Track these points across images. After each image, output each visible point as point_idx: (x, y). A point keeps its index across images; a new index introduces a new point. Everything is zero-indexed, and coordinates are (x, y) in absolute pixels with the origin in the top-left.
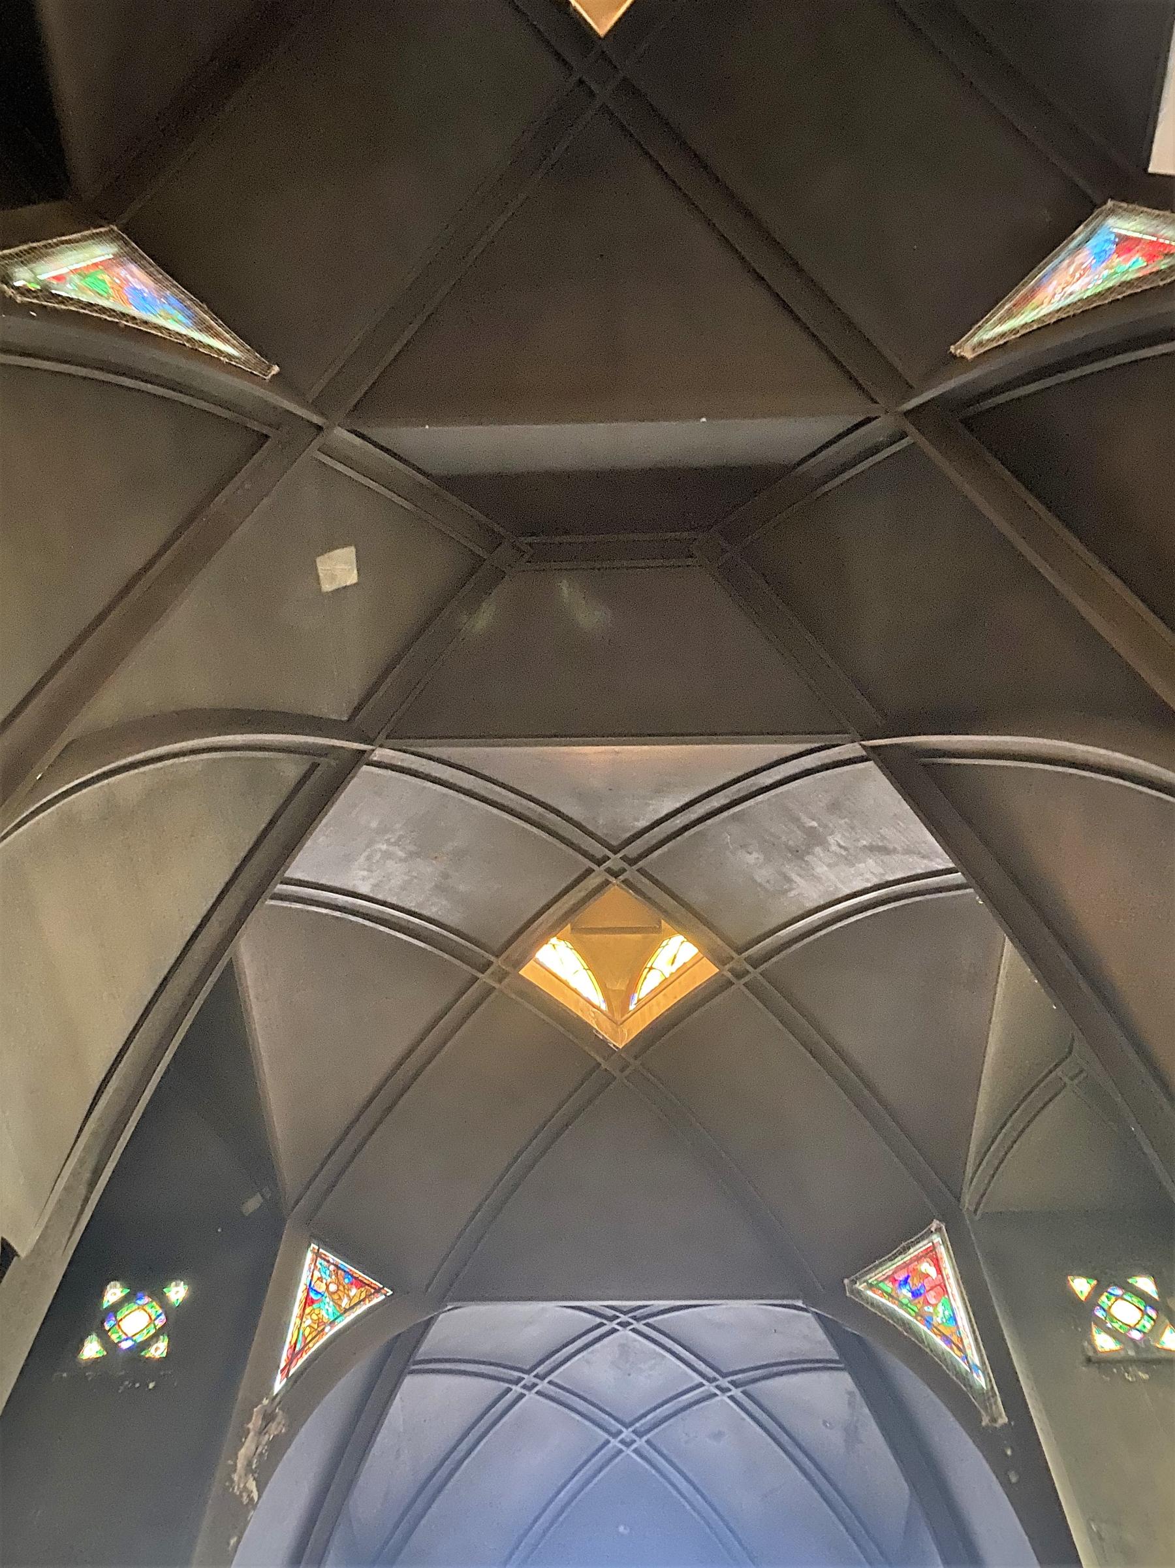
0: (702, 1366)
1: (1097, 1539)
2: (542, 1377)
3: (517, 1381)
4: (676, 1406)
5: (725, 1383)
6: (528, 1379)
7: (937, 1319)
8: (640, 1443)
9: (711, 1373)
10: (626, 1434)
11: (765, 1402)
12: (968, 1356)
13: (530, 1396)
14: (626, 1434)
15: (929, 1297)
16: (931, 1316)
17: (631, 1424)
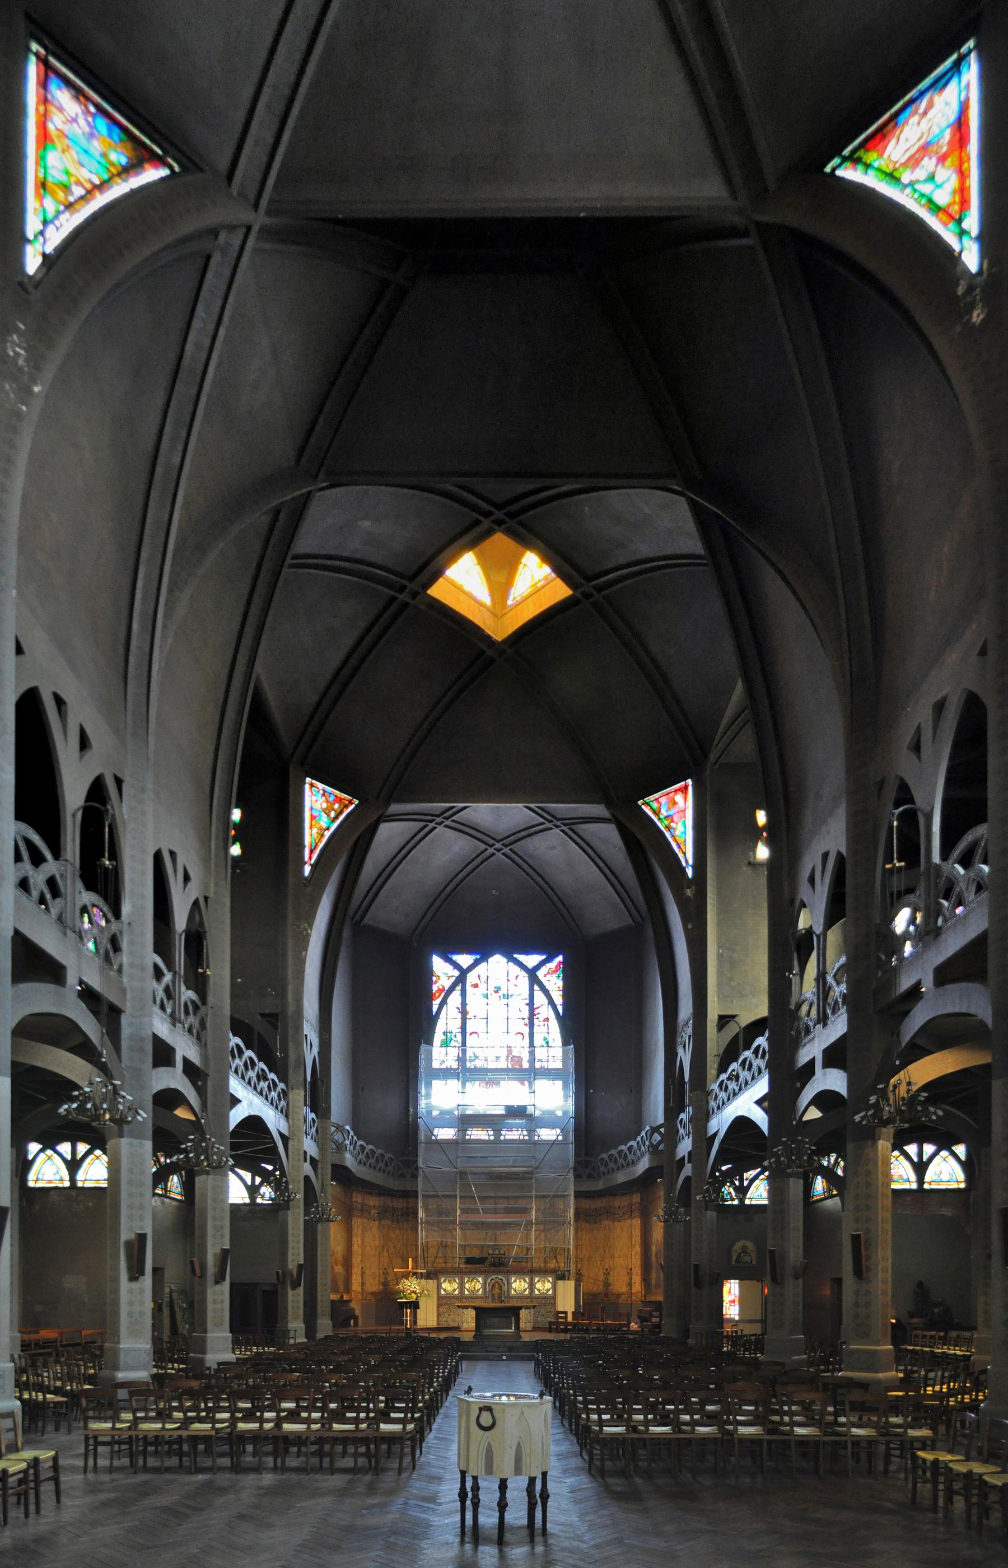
0: (545, 815)
1: (720, 957)
2: (447, 818)
3: (431, 821)
4: (528, 832)
5: (558, 823)
6: (439, 820)
7: (677, 833)
8: (506, 850)
9: (550, 818)
10: (498, 845)
11: (581, 834)
12: (687, 856)
13: (440, 829)
14: (498, 845)
15: (675, 813)
16: (675, 829)
17: (502, 840)
